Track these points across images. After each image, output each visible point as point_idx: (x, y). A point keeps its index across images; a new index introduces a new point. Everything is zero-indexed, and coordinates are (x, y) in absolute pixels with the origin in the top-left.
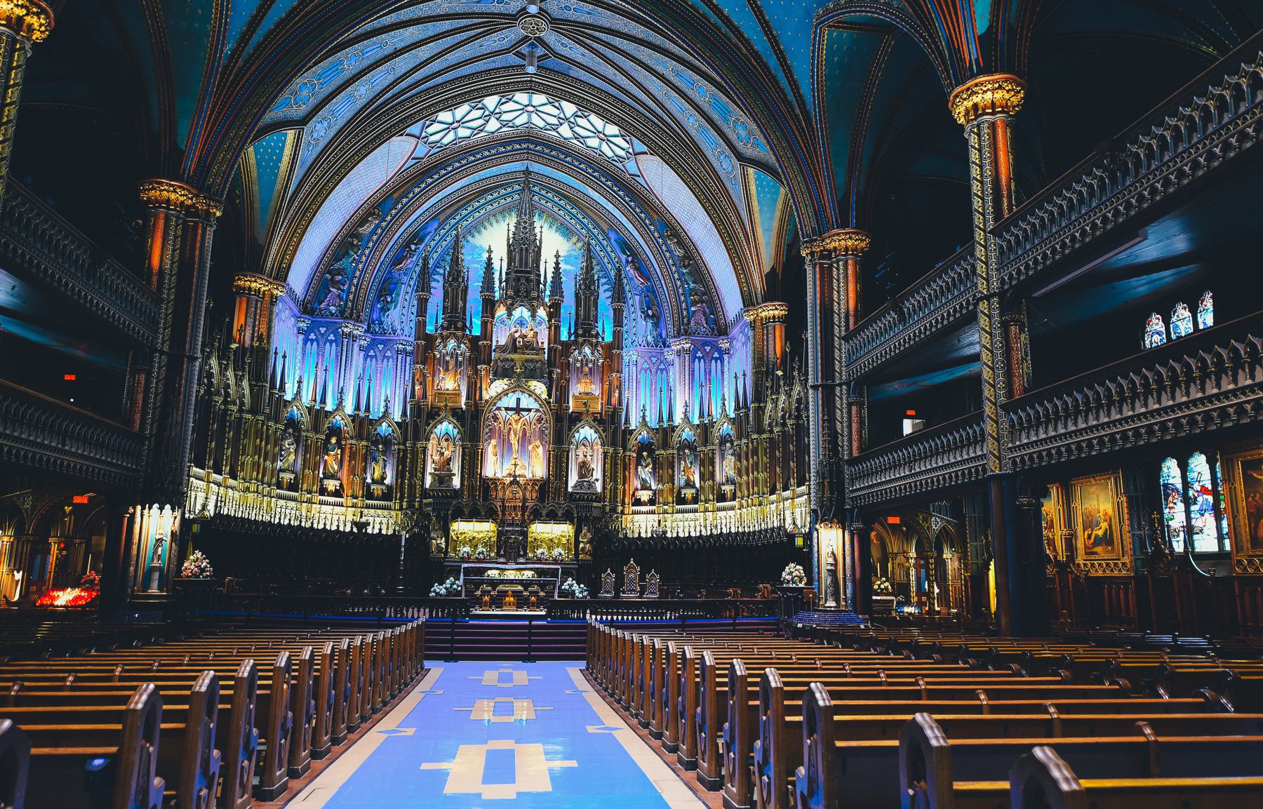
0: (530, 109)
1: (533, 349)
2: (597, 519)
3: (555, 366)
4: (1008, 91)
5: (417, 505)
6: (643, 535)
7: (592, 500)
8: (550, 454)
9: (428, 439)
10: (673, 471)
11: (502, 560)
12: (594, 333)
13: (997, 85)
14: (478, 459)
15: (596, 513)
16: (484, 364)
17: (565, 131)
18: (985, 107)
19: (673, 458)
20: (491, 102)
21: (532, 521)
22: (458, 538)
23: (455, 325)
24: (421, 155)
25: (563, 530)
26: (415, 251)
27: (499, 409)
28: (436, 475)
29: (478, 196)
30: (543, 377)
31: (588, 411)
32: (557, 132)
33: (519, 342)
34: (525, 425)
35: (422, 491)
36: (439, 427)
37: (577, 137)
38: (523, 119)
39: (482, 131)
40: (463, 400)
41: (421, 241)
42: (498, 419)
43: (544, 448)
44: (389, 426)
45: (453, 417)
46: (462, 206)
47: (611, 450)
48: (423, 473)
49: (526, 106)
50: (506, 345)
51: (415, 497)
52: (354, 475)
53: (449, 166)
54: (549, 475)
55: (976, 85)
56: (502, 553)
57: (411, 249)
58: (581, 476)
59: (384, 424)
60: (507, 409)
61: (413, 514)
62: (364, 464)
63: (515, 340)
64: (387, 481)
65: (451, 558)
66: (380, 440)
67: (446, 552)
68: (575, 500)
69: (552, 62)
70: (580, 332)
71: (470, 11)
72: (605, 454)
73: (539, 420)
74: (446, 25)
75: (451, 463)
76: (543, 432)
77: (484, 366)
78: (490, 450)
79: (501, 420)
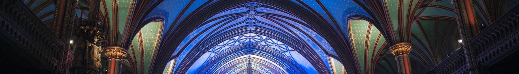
0: (250, 37)
4: (406, 47)
13: (402, 46)
17: (263, 43)
18: (400, 52)
20: (236, 38)
24: (212, 57)
32: (260, 44)
37: (268, 45)
38: (248, 40)
39: (233, 46)
49: (249, 37)
53: (222, 59)
55: (396, 46)
69: (258, 24)
71: (231, 14)
74: (223, 19)
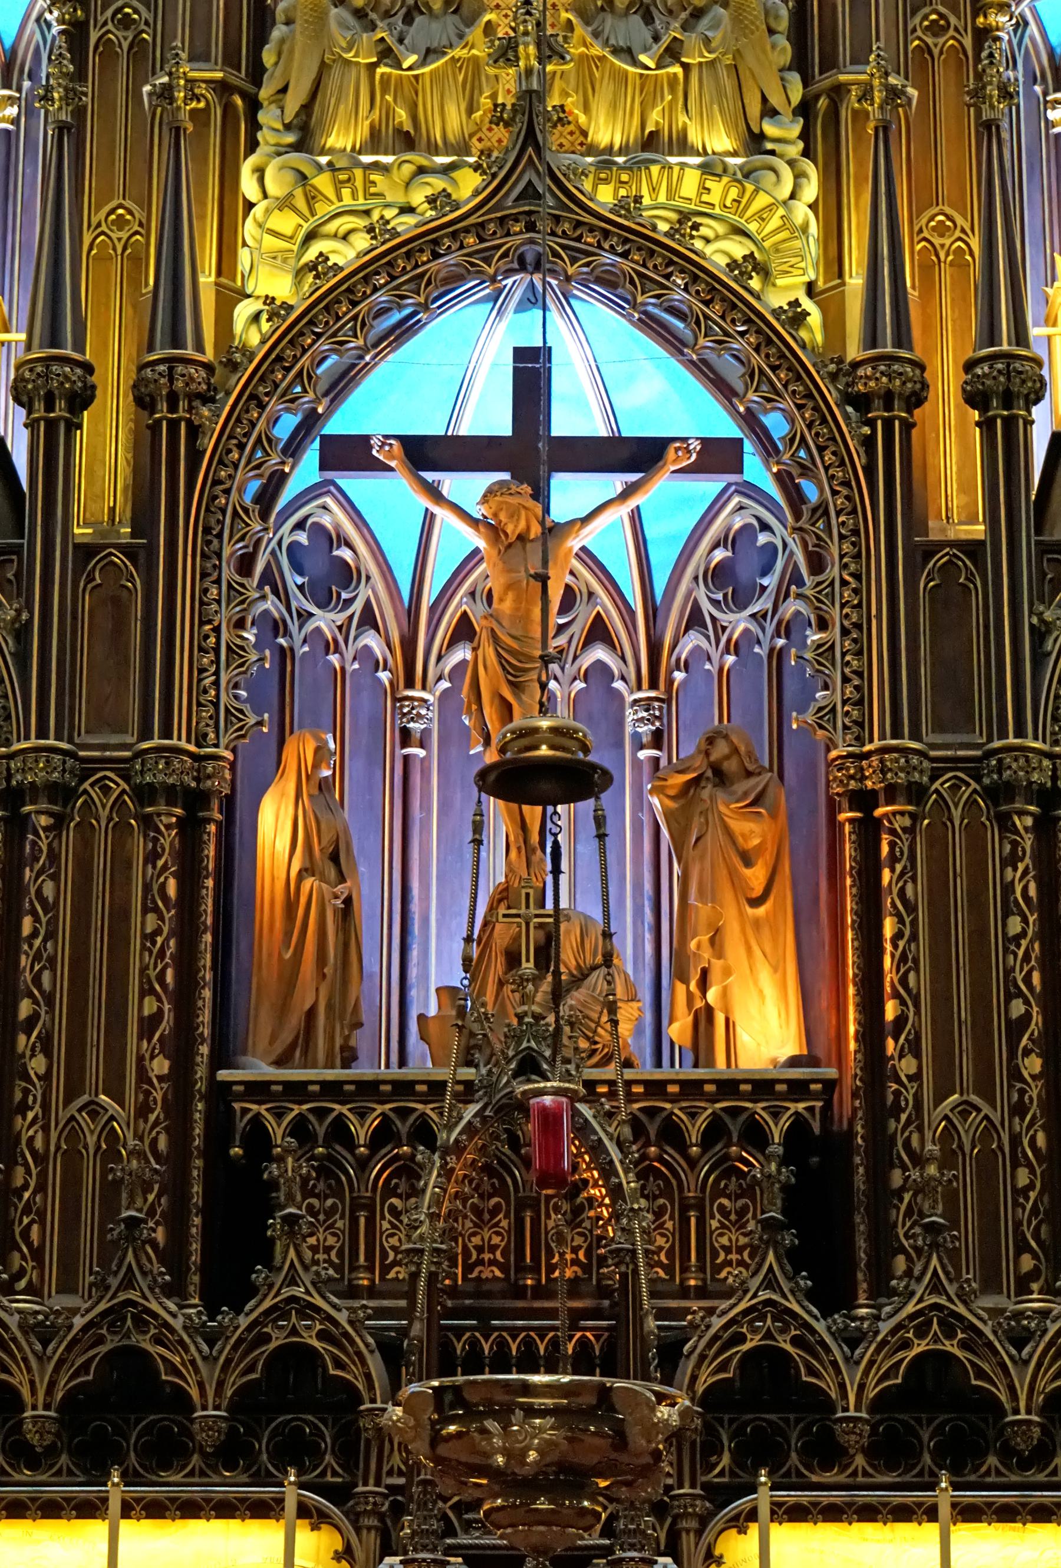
16: (199, 56)
34: (599, 632)
42: (347, 575)
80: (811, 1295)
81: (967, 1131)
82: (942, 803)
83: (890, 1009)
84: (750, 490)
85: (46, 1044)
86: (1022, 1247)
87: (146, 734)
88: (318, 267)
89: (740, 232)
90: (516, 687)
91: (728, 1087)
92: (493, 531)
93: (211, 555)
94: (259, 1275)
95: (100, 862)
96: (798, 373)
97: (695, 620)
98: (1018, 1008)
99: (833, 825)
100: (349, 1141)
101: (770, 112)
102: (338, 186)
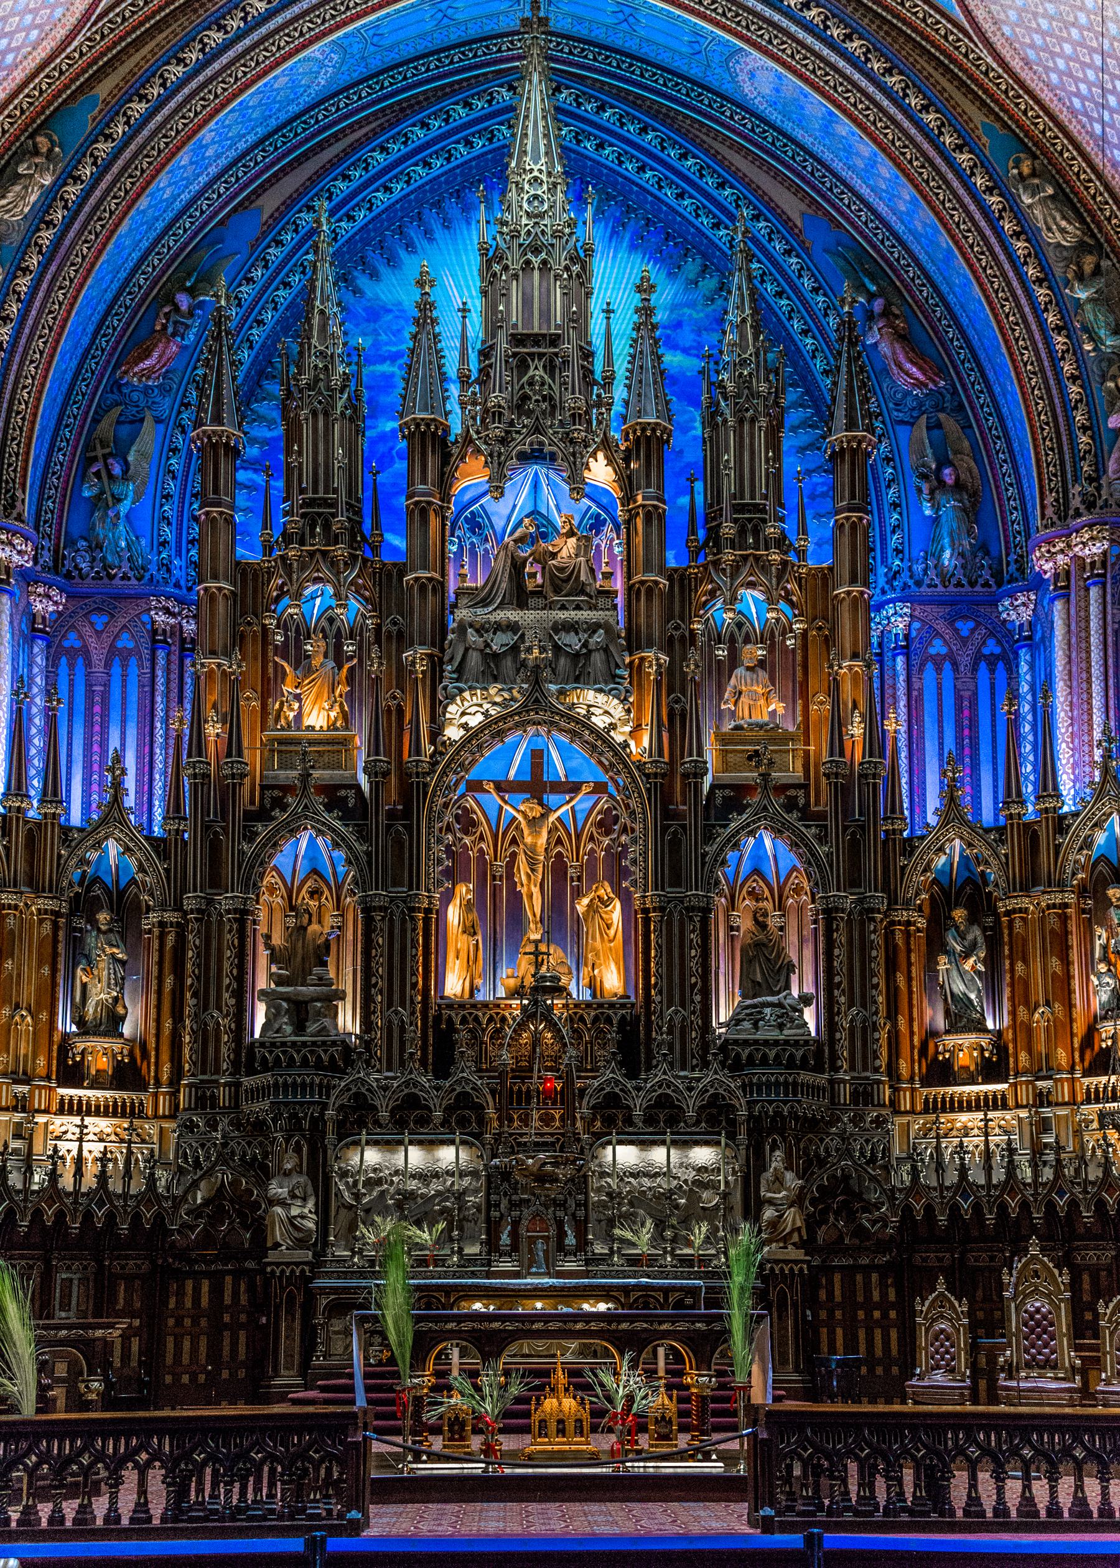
1: (582, 592)
2: (812, 1125)
3: (650, 646)
5: (223, 1096)
6: (977, 1176)
7: (791, 1064)
8: (647, 921)
9: (250, 883)
10: (1067, 963)
11: (506, 1266)
12: (770, 531)
14: (414, 946)
15: (809, 1106)
19: (1064, 919)
21: (601, 1139)
22: (357, 1196)
23: (327, 527)
25: (703, 1155)
26: (191, 314)
27: (476, 786)
28: (287, 999)
29: (383, 129)
30: (614, 678)
31: (765, 776)
33: (533, 575)
34: (559, 842)
35: (237, 1051)
36: (287, 848)
40: (361, 758)
41: (207, 279)
42: (474, 824)
43: (625, 898)
44: (128, 849)
45: (329, 808)
46: (333, 164)
47: (849, 901)
48: (240, 994)
50: (492, 581)
51: (217, 1071)
52: (17, 1006)
54: (647, 987)
56: (505, 1239)
57: (177, 309)
58: (751, 987)
59: (113, 848)
60: (501, 787)
61: (213, 1125)
62: (46, 971)
63: (517, 566)
64: (127, 1029)
65: (341, 1261)
66: (104, 899)
67: (321, 1245)
68: (737, 1067)
70: (728, 529)
72: (829, 914)
73: (606, 824)
75: (331, 960)
76: (615, 857)
77: (422, 650)
78: (453, 914)
79: (484, 828)
80: (625, 1075)
81: (678, 1019)
82: (671, 913)
83: (653, 980)
84: (611, 796)
85: (381, 992)
86: (693, 1057)
87: (411, 889)
88: (465, 726)
89: (606, 712)
90: (533, 870)
91: (600, 1006)
92: (524, 813)
93: (430, 827)
94: (452, 1069)
95: (397, 931)
96: (626, 766)
97: (592, 838)
98: (693, 980)
99: (636, 919)
100: (480, 1024)
101: (618, 666)
102: (472, 695)
